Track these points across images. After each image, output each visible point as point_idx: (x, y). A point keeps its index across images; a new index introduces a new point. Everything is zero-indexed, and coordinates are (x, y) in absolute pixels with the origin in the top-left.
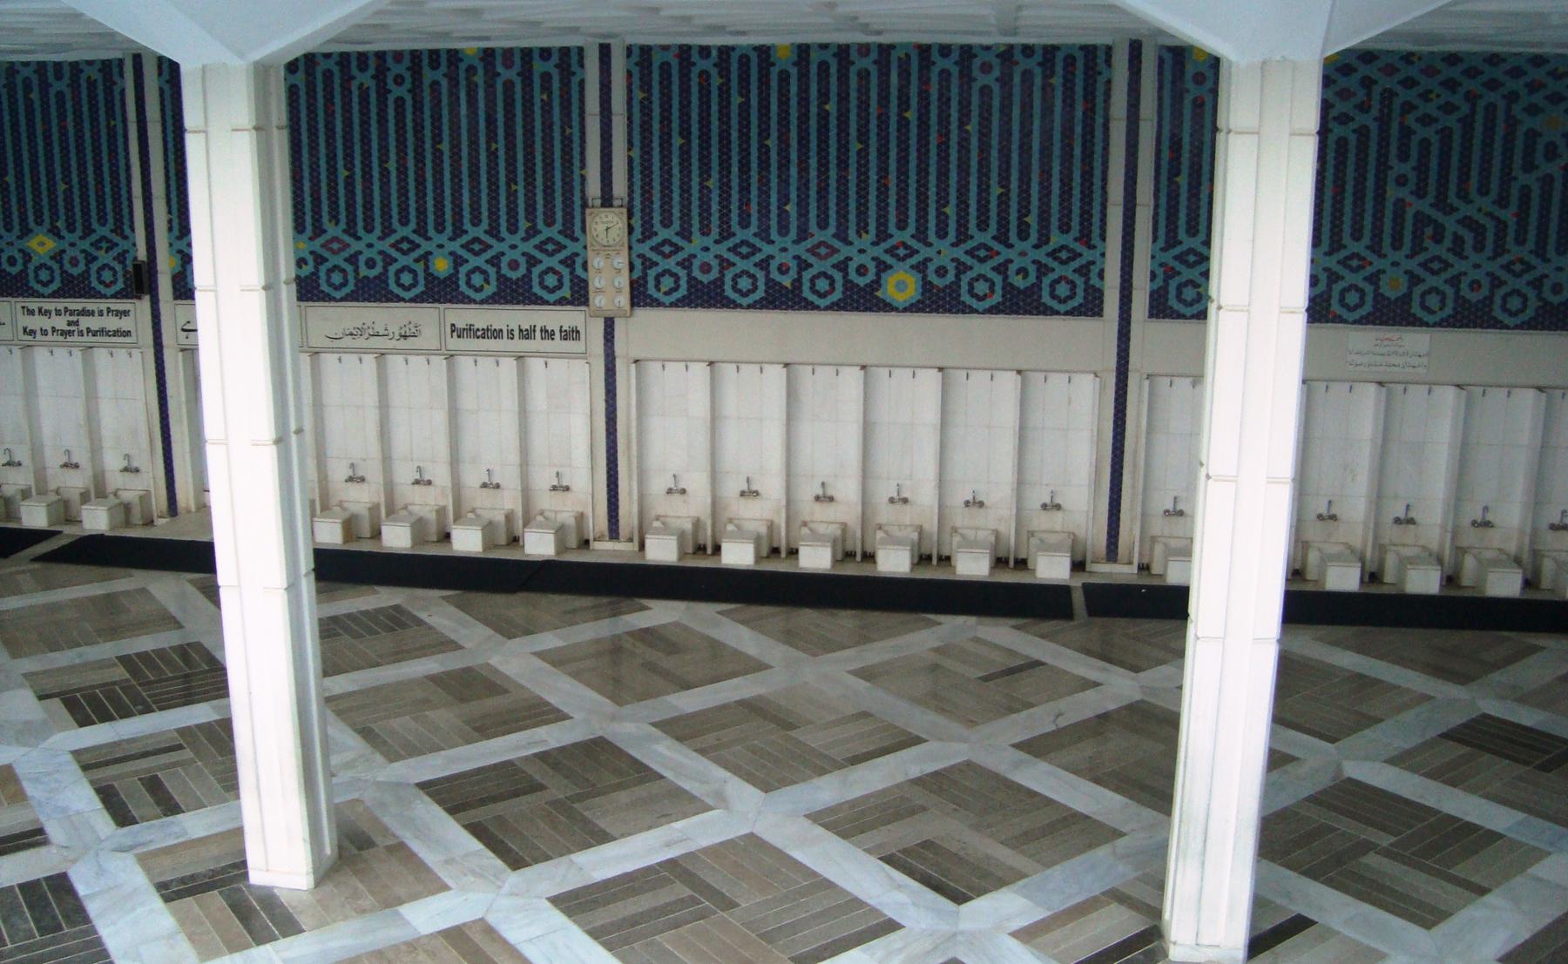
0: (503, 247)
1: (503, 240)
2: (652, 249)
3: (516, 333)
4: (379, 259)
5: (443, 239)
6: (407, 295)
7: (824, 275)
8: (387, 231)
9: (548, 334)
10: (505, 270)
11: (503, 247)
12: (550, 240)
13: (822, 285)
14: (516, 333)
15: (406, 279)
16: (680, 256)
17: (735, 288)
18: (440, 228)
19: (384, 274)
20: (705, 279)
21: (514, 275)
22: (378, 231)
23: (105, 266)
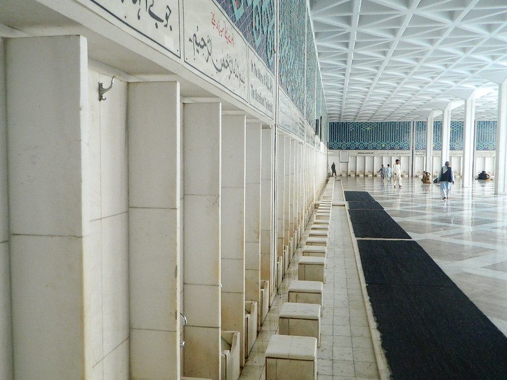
9: (369, 153)
18: (357, 141)
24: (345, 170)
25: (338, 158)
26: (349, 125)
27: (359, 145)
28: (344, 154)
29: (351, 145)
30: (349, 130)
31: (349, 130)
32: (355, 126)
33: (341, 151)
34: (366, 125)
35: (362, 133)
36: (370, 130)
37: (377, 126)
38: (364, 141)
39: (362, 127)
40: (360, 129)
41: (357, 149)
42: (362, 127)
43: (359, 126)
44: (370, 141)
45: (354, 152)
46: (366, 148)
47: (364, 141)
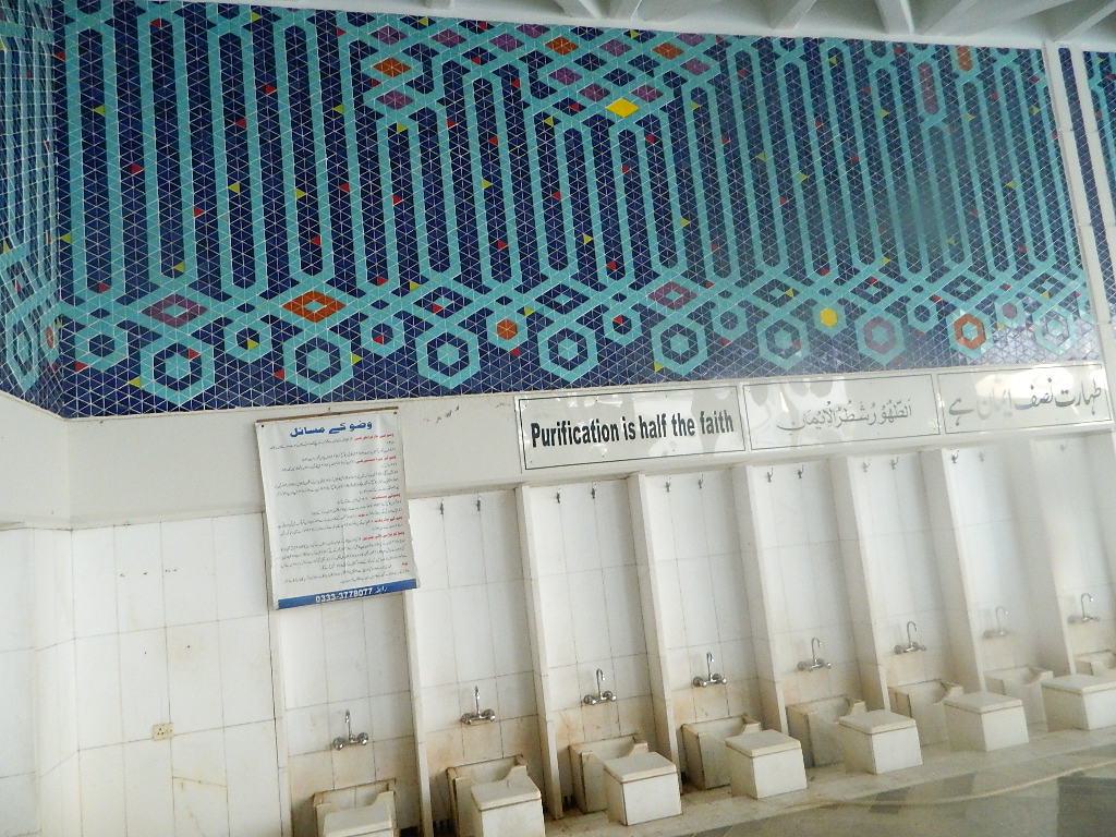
0: (488, 301)
1: (603, 287)
2: (585, 299)
3: (637, 428)
4: (635, 317)
5: (728, 283)
6: (180, 398)
7: (679, 328)
8: (532, 277)
10: (610, 333)
11: (488, 301)
12: (561, 289)
13: (680, 344)
14: (637, 428)
15: (569, 350)
16: (583, 310)
17: (301, 368)
19: (408, 351)
20: (623, 340)
21: (384, 350)
22: (517, 277)
23: (878, 321)
24: (373, 716)
25: (233, 533)
26: (361, 51)
27: (536, 322)
28: (326, 467)
29: (414, 326)
30: (368, 119)
31: (368, 119)
32: (453, 72)
33: (272, 430)
34: (591, 62)
35: (547, 160)
36: (650, 124)
37: (721, 84)
38: (588, 274)
39: (541, 91)
40: (515, 106)
41: (513, 371)
42: (541, 91)
43: (509, 75)
44: (668, 258)
45: (480, 430)
46: (621, 366)
47: (588, 274)
